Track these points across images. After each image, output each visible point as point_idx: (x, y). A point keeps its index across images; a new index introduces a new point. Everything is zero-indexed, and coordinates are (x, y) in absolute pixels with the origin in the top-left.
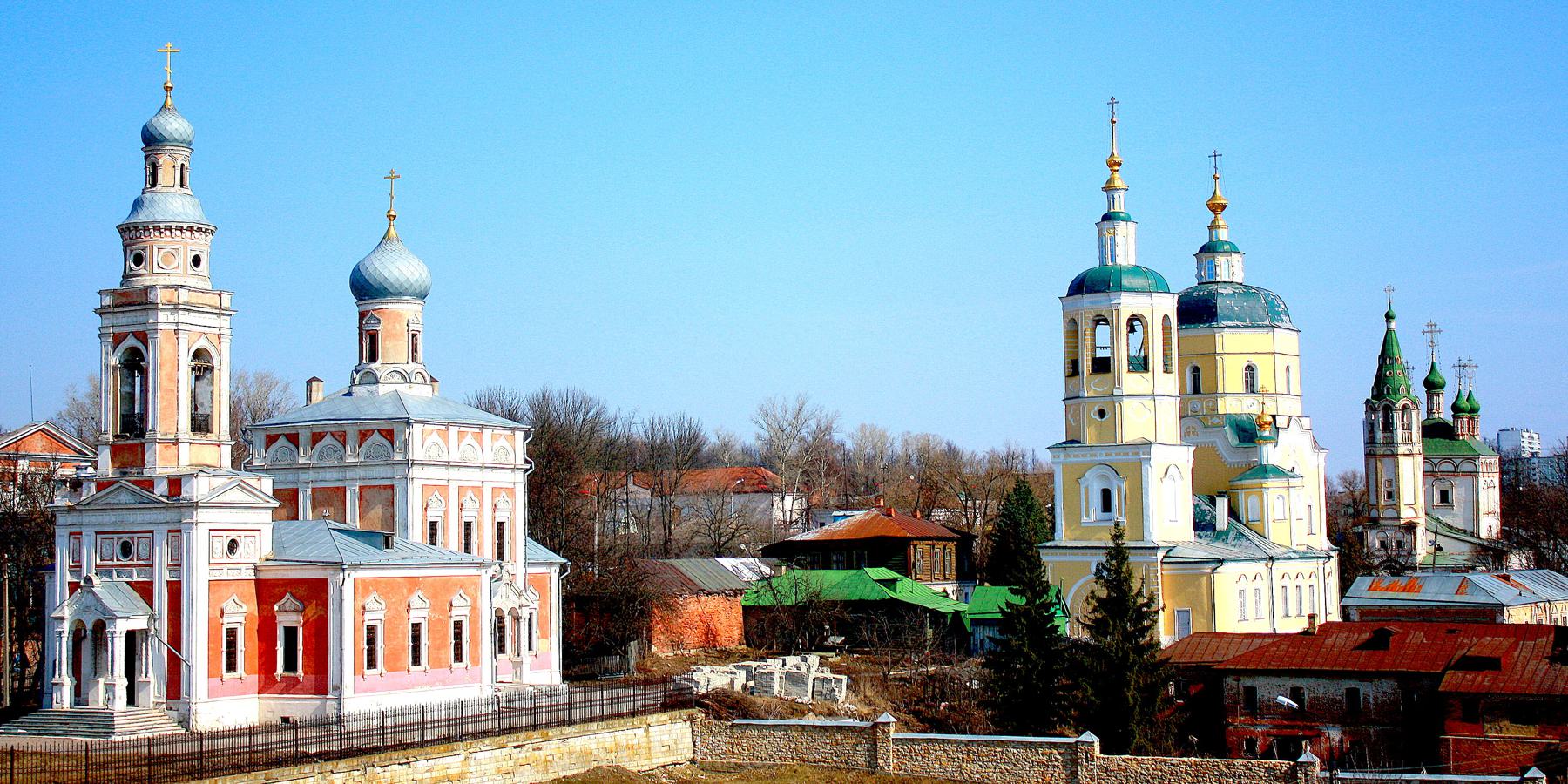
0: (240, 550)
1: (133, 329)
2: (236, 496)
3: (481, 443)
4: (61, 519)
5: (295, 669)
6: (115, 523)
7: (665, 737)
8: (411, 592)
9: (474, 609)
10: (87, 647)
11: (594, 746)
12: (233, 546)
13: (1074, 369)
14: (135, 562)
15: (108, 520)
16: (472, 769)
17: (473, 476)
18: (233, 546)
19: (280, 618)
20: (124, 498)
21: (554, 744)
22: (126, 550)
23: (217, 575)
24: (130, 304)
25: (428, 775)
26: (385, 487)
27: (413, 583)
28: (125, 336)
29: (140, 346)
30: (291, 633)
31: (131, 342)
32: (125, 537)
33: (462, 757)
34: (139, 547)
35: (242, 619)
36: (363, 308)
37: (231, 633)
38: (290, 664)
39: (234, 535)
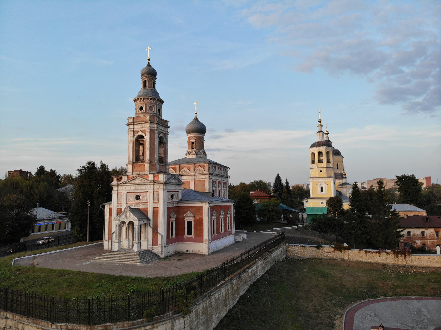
0: (174, 198)
2: (174, 181)
3: (221, 170)
4: (115, 189)
5: (191, 234)
6: (134, 190)
8: (220, 210)
9: (231, 214)
10: (124, 229)
13: (313, 162)
14: (141, 202)
15: (131, 188)
17: (220, 179)
20: (137, 181)
22: (138, 198)
24: (139, 122)
26: (202, 181)
28: (138, 132)
30: (189, 223)
31: (140, 133)
32: (138, 194)
36: (189, 136)
37: (172, 223)
38: (189, 233)
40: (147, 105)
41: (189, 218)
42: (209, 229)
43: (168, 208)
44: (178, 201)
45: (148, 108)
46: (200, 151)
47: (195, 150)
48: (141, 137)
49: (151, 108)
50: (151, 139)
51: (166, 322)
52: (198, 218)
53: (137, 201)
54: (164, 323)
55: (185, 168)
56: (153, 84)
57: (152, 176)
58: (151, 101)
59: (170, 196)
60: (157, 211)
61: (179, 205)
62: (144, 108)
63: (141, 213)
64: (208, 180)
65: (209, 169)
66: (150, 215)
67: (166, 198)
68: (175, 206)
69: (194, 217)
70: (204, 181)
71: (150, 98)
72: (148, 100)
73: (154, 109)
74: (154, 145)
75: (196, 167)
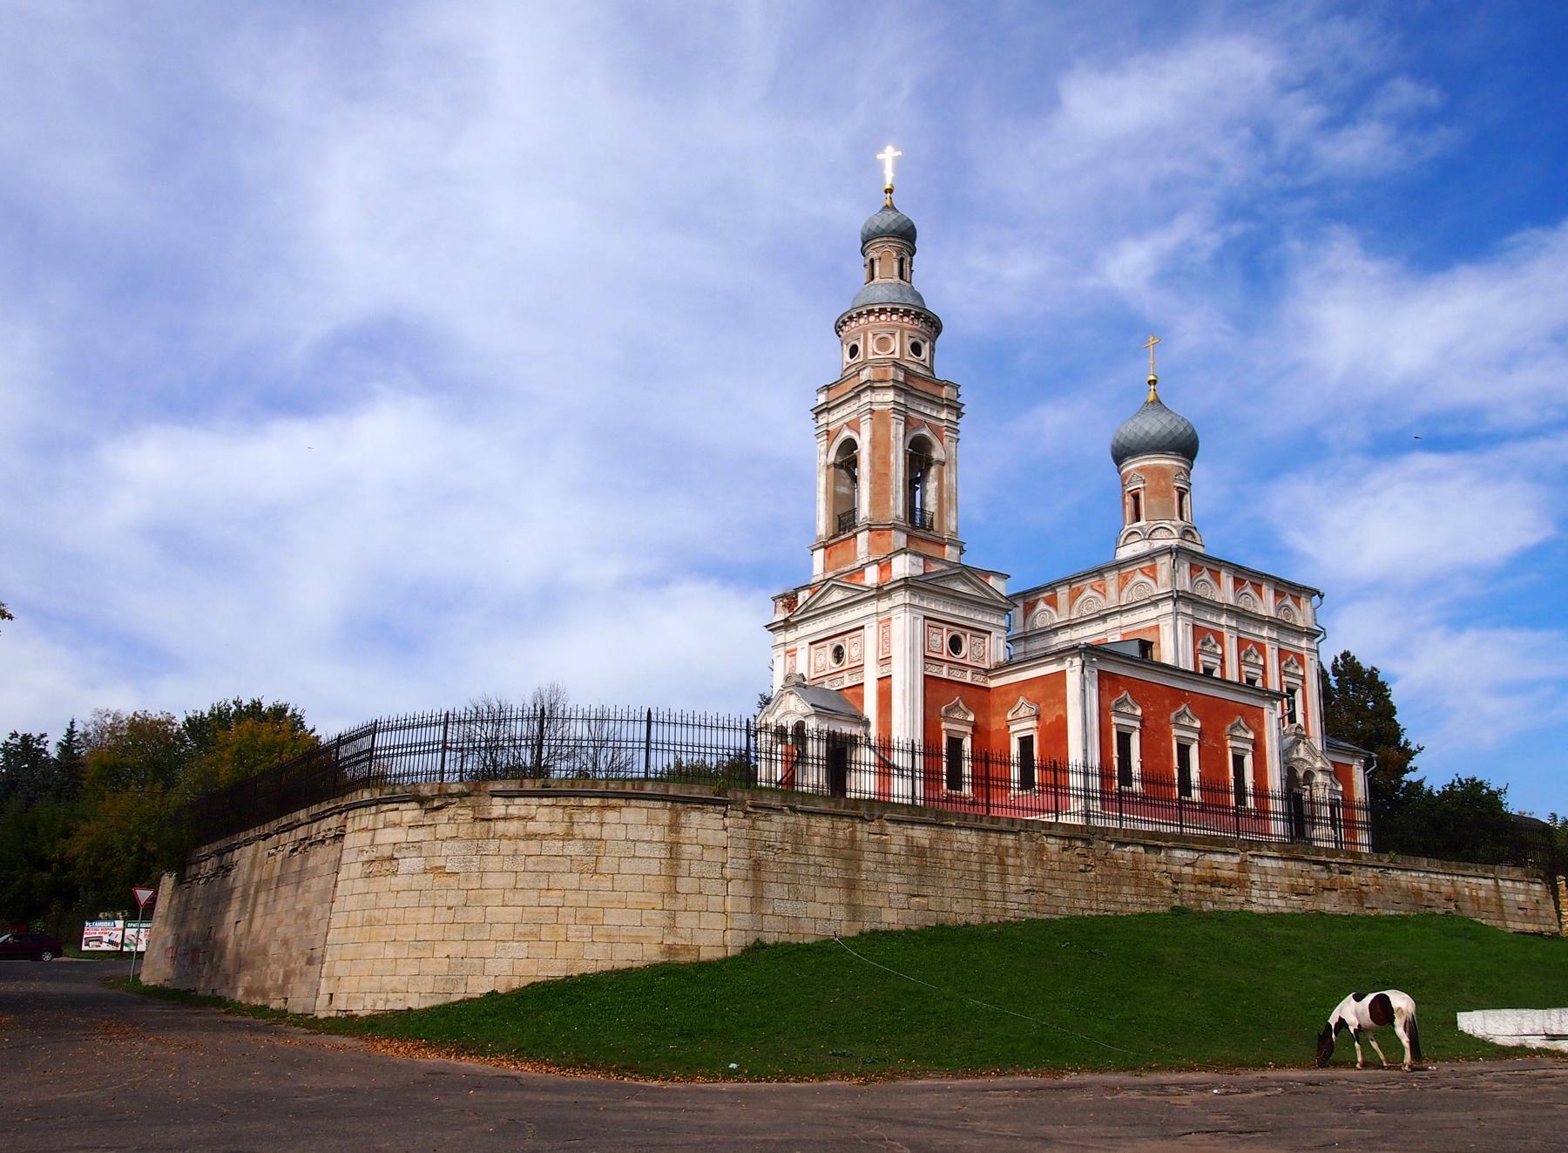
1: (847, 420)
7: (1521, 898)
11: (1425, 887)
12: (955, 644)
16: (1255, 877)
18: (955, 644)
19: (1013, 728)
20: (836, 596)
21: (1370, 872)
22: (838, 653)
23: (933, 671)
25: (1188, 870)
27: (1178, 696)
28: (840, 431)
29: (854, 435)
30: (1026, 743)
31: (846, 433)
33: (1236, 860)
34: (851, 652)
35: (969, 730)
37: (955, 743)
39: (957, 631)
40: (870, 335)
41: (1021, 725)
42: (1085, 751)
43: (927, 678)
44: (987, 666)
45: (872, 345)
46: (1166, 524)
47: (1142, 523)
48: (849, 446)
49: (883, 343)
50: (874, 443)
51: (651, 804)
52: (1050, 718)
53: (837, 668)
54: (643, 803)
55: (1088, 593)
56: (896, 265)
57: (875, 568)
58: (883, 317)
59: (941, 639)
60: (890, 687)
61: (993, 684)
62: (861, 348)
63: (843, 704)
64: (1170, 620)
65: (1173, 579)
66: (870, 709)
67: (919, 641)
68: (968, 680)
69: (1038, 717)
70: (1157, 627)
71: (876, 308)
72: (872, 318)
73: (895, 345)
74: (886, 463)
75: (1125, 578)
